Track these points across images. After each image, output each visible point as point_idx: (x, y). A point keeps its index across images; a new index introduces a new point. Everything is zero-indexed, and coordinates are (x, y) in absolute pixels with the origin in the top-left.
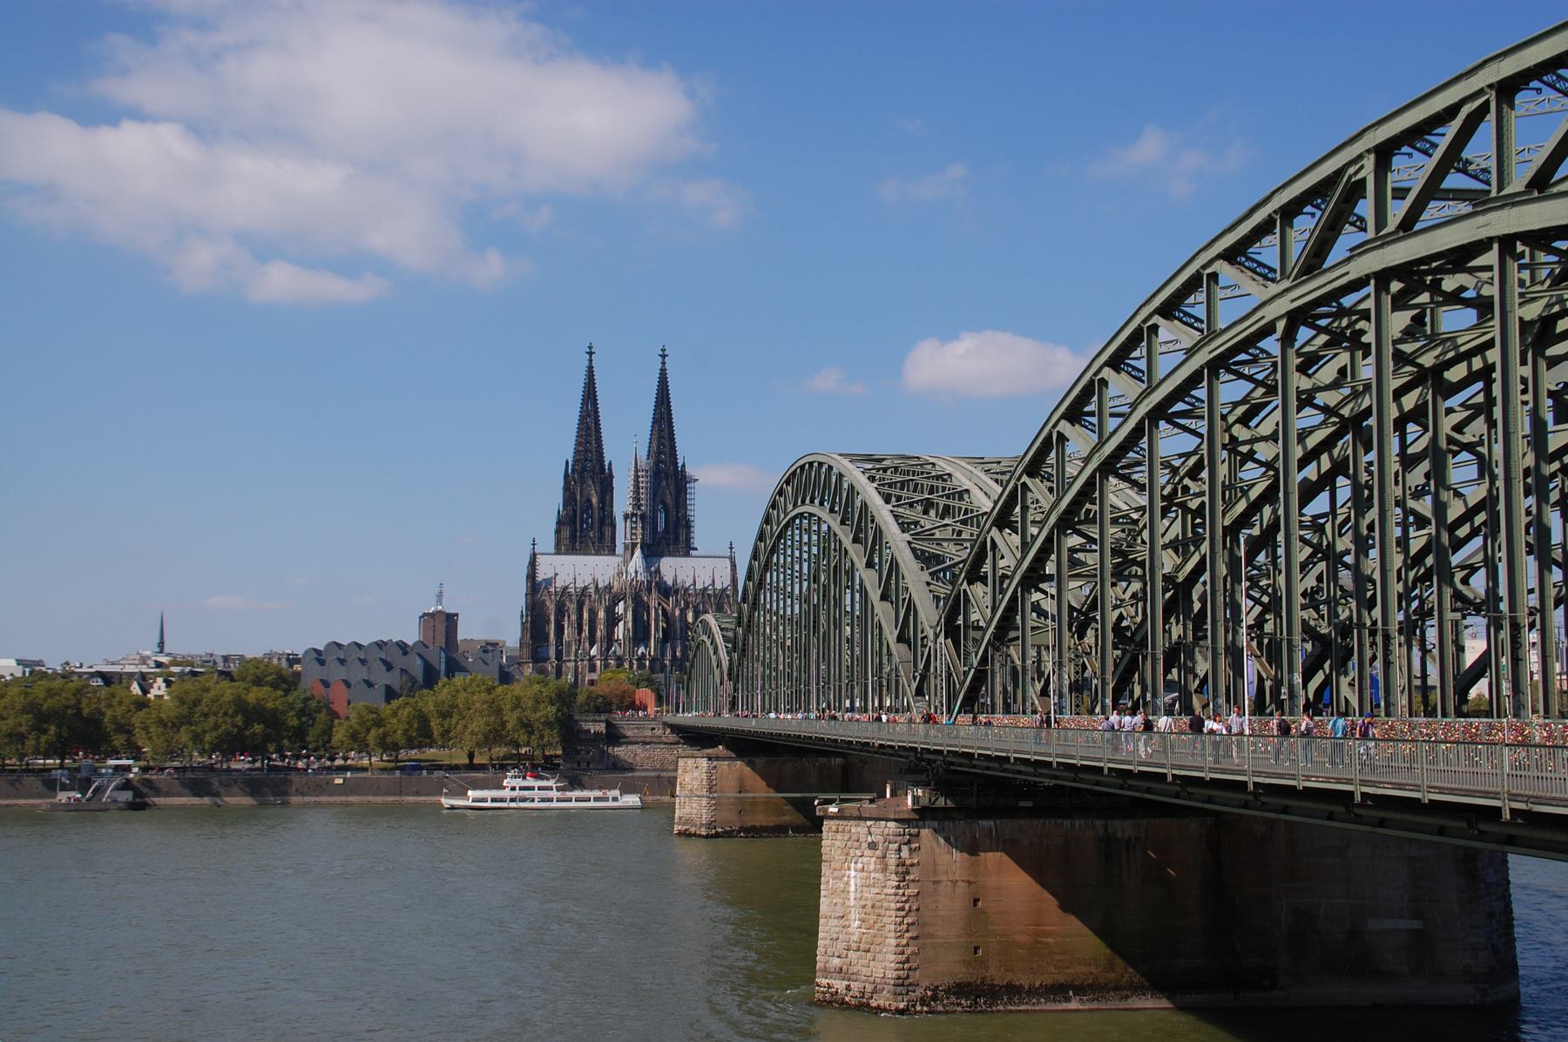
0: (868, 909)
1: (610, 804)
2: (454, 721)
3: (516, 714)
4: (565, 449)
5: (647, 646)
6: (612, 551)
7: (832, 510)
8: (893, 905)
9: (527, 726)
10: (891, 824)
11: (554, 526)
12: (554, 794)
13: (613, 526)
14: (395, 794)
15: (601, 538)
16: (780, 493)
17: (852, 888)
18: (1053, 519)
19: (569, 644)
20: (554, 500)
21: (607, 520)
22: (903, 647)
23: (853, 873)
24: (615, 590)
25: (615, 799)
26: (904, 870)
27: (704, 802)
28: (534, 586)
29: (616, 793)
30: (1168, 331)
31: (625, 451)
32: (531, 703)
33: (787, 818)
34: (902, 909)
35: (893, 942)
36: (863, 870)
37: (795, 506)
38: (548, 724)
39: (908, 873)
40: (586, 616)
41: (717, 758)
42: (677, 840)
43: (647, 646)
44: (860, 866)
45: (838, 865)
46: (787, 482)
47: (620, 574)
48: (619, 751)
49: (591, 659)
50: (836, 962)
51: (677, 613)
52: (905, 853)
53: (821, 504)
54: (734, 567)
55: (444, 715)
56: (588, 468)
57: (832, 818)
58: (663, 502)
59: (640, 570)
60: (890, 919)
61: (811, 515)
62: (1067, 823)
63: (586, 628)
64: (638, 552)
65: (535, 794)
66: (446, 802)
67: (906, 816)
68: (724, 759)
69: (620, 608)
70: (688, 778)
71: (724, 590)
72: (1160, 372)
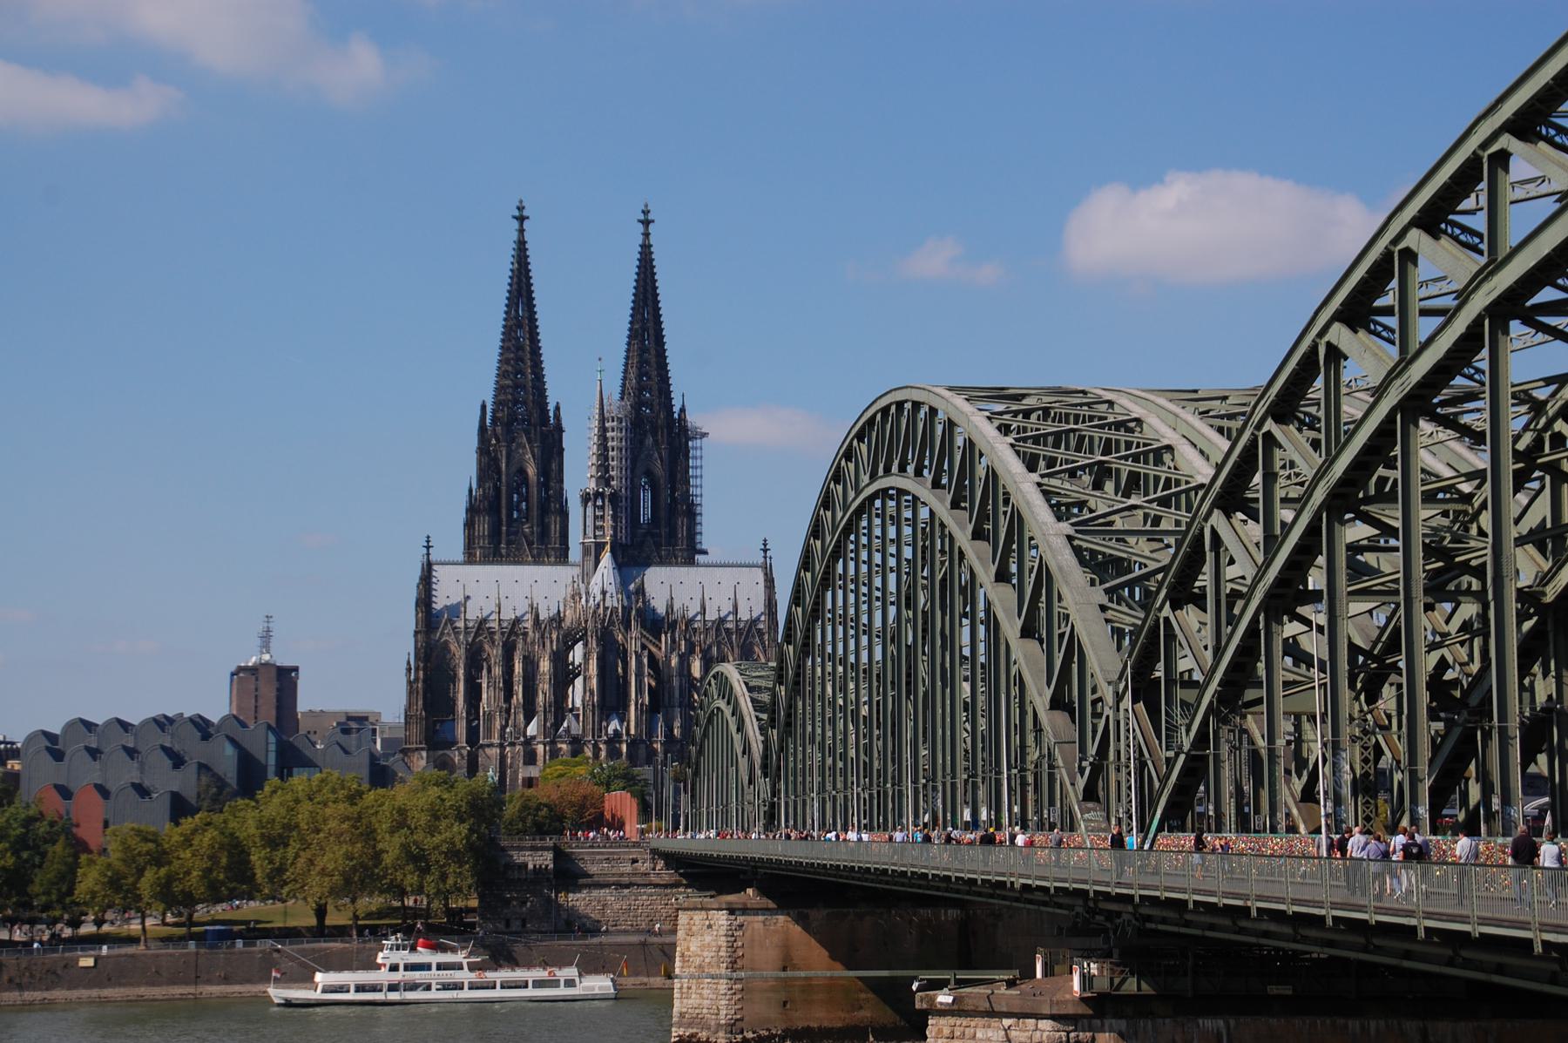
2: (291, 852)
3: (398, 839)
4: (480, 382)
5: (623, 719)
7: (936, 484)
9: (417, 858)
10: (1046, 1025)
11: (461, 516)
13: (564, 514)
14: (185, 982)
15: (544, 534)
16: (849, 454)
18: (1319, 495)
19: (490, 717)
20: (463, 471)
21: (552, 504)
22: (1061, 717)
24: (567, 624)
25: (570, 983)
27: (723, 986)
28: (429, 618)
30: (1525, 161)
31: (584, 384)
32: (424, 819)
33: (865, 1014)
37: (874, 477)
38: (453, 854)
40: (518, 668)
41: (745, 910)
43: (623, 719)
46: (860, 436)
47: (576, 596)
48: (578, 900)
49: (529, 742)
51: (674, 661)
53: (918, 473)
54: (770, 583)
55: (274, 842)
56: (519, 418)
57: (943, 1012)
58: (649, 473)
59: (611, 589)
61: (901, 492)
62: (1354, 1025)
63: (519, 689)
64: (606, 559)
66: (277, 993)
67: (1070, 1010)
68: (756, 911)
69: (577, 654)
71: (754, 622)
72: (1513, 233)
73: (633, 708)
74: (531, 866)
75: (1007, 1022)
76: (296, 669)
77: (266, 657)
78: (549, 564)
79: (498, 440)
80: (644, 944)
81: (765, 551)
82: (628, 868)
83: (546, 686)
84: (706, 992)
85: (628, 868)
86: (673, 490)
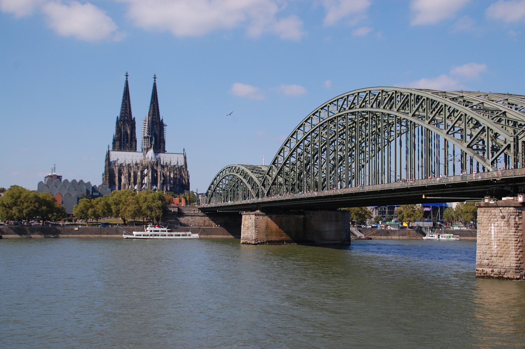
0: (501, 241)
1: (188, 237)
2: (121, 206)
3: (146, 204)
4: (117, 112)
5: (157, 186)
6: (135, 150)
8: (513, 239)
9: (150, 208)
10: (512, 209)
12: (167, 233)
14: (98, 234)
17: (493, 233)
20: (112, 131)
21: (133, 139)
23: (493, 228)
25: (190, 235)
26: (517, 225)
27: (254, 231)
28: (109, 163)
29: (190, 233)
32: (151, 200)
33: (283, 238)
34: (516, 240)
35: (514, 253)
36: (498, 226)
38: (159, 208)
39: (518, 227)
41: (259, 215)
42: (242, 246)
43: (157, 186)
44: (496, 225)
45: (485, 225)
48: (182, 220)
50: (486, 261)
51: (168, 174)
52: (517, 219)
54: (185, 158)
55: (116, 204)
59: (153, 157)
60: (512, 245)
65: (160, 233)
66: (125, 236)
67: (518, 205)
68: (261, 215)
69: (146, 171)
70: (246, 222)
71: (182, 166)
75: (501, 208)
77: (54, 174)
80: (199, 228)
82: (193, 212)
85: (193, 212)
86: (160, 137)
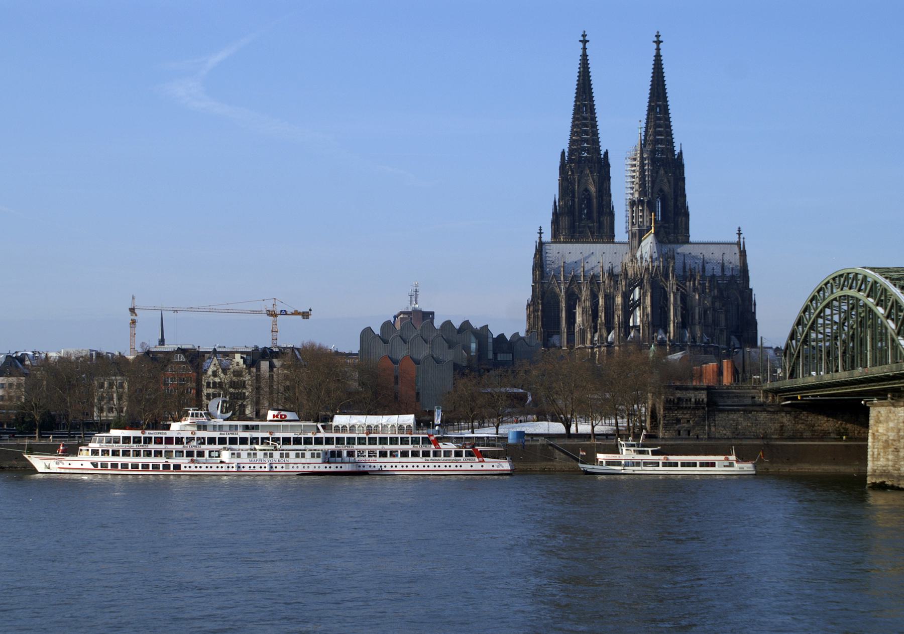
11: (550, 217)
15: (600, 226)
19: (583, 332)
31: (621, 137)
40: (601, 302)
43: (666, 331)
54: (743, 254)
58: (661, 190)
63: (602, 315)
70: (881, 429)
73: (672, 325)
74: (693, 400)
76: (433, 313)
78: (603, 243)
79: (572, 172)
81: (739, 234)
83: (620, 312)
84: (890, 457)
